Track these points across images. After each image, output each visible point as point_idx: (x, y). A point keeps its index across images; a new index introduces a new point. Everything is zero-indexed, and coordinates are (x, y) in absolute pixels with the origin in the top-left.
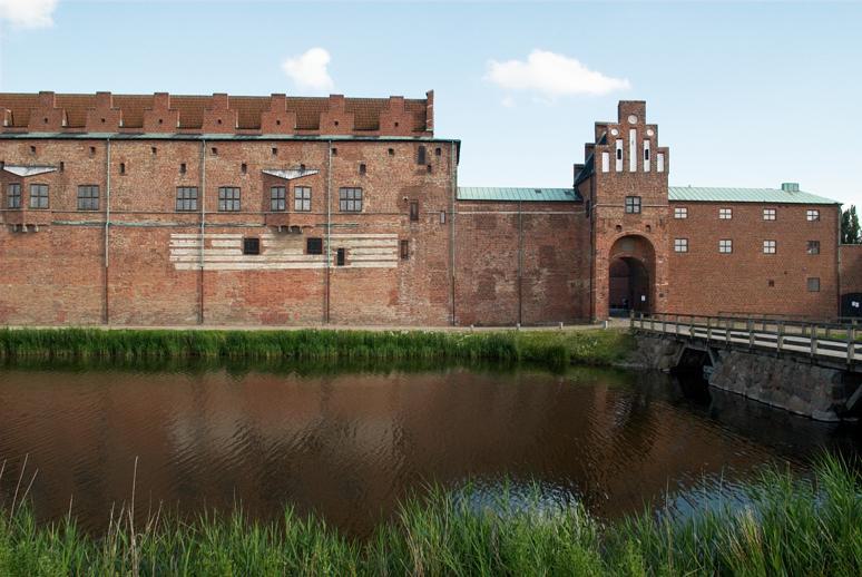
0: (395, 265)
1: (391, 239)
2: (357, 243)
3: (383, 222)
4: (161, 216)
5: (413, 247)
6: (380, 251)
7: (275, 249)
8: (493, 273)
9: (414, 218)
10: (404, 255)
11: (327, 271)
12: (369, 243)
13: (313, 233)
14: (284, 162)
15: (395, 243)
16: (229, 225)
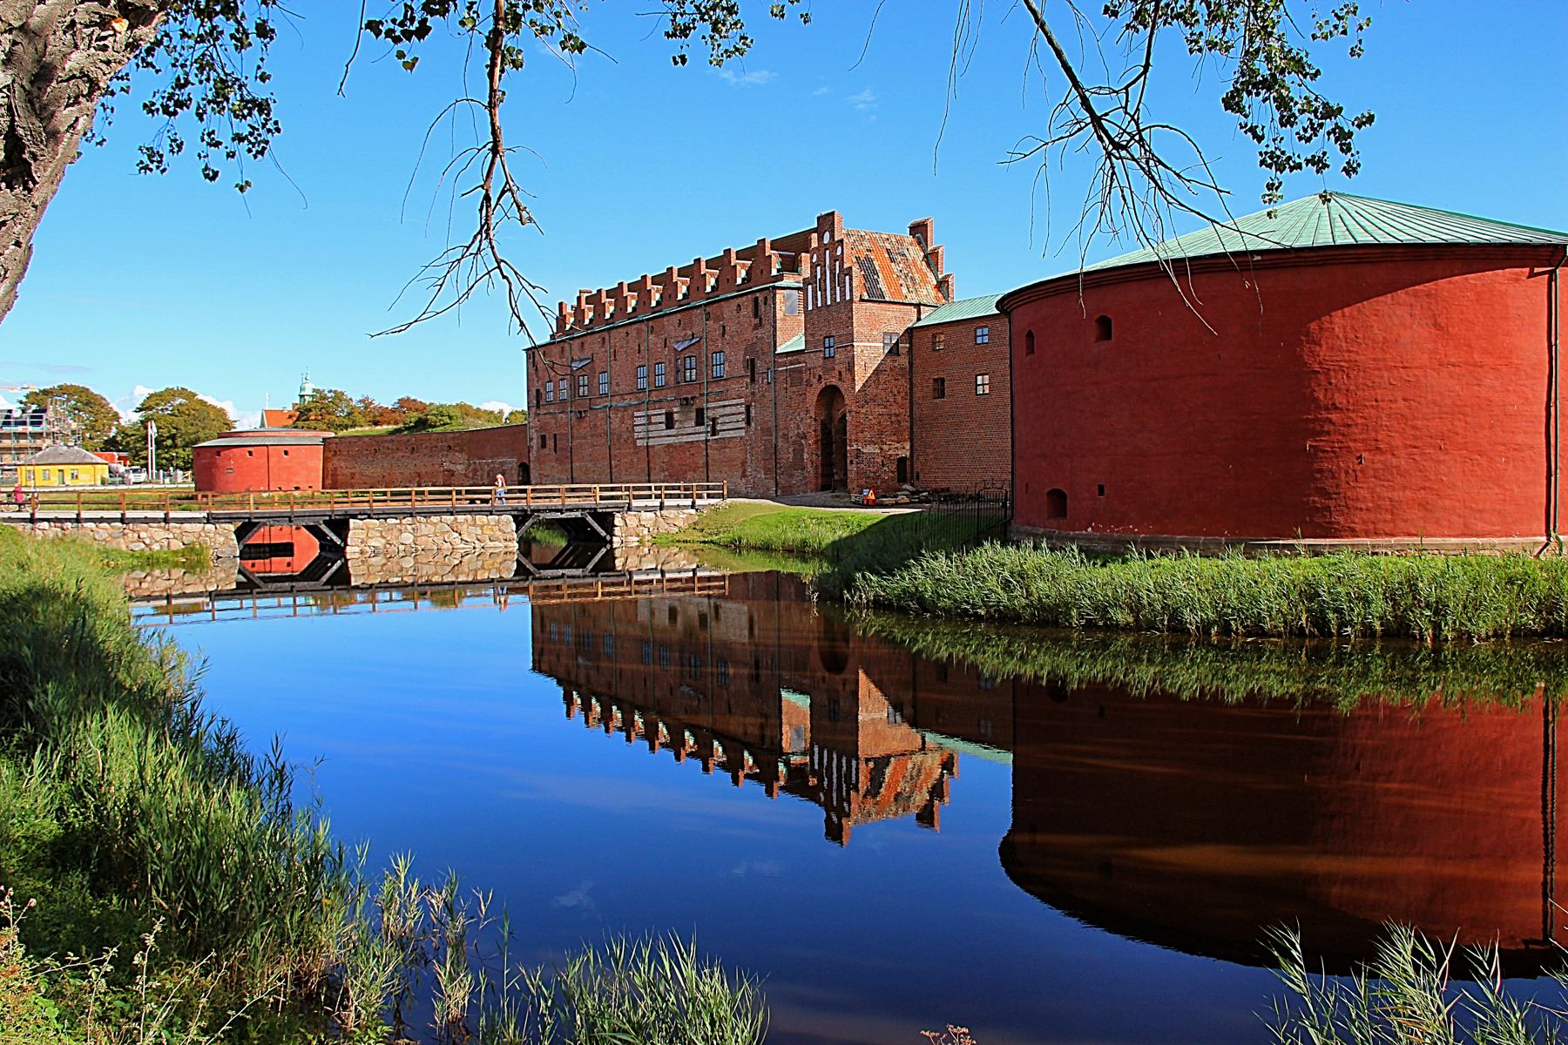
0: (742, 433)
1: (741, 404)
2: (721, 411)
3: (735, 387)
4: (631, 396)
5: (753, 411)
6: (734, 418)
7: (681, 422)
8: (802, 438)
9: (753, 380)
10: (748, 421)
11: (707, 441)
12: (728, 410)
13: (698, 404)
14: (684, 332)
15: (743, 409)
16: (660, 401)
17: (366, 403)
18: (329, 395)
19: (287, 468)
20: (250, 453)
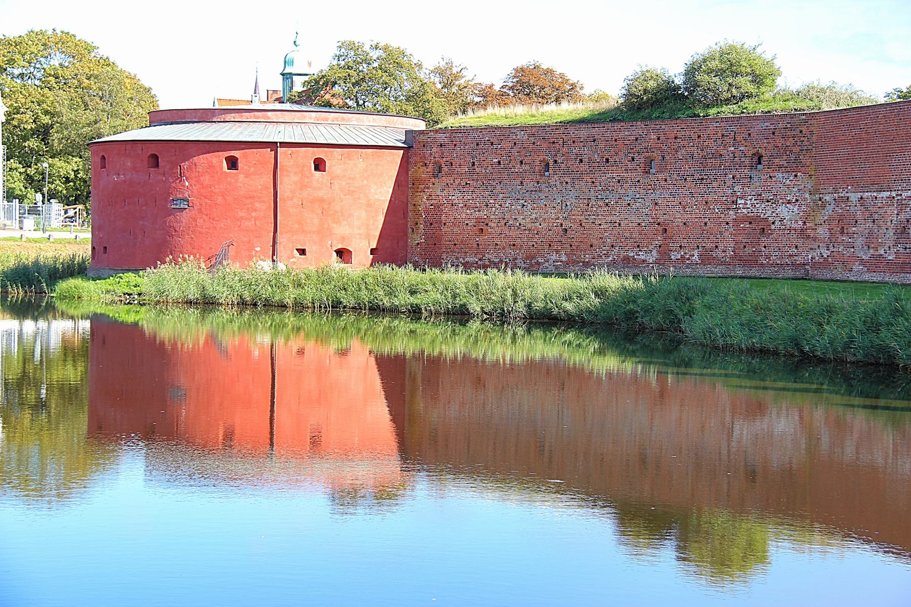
17: (448, 76)
18: (374, 54)
19: (322, 200)
20: (233, 163)
